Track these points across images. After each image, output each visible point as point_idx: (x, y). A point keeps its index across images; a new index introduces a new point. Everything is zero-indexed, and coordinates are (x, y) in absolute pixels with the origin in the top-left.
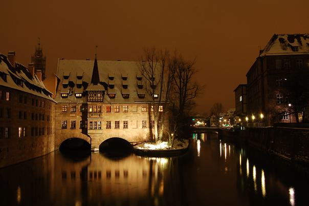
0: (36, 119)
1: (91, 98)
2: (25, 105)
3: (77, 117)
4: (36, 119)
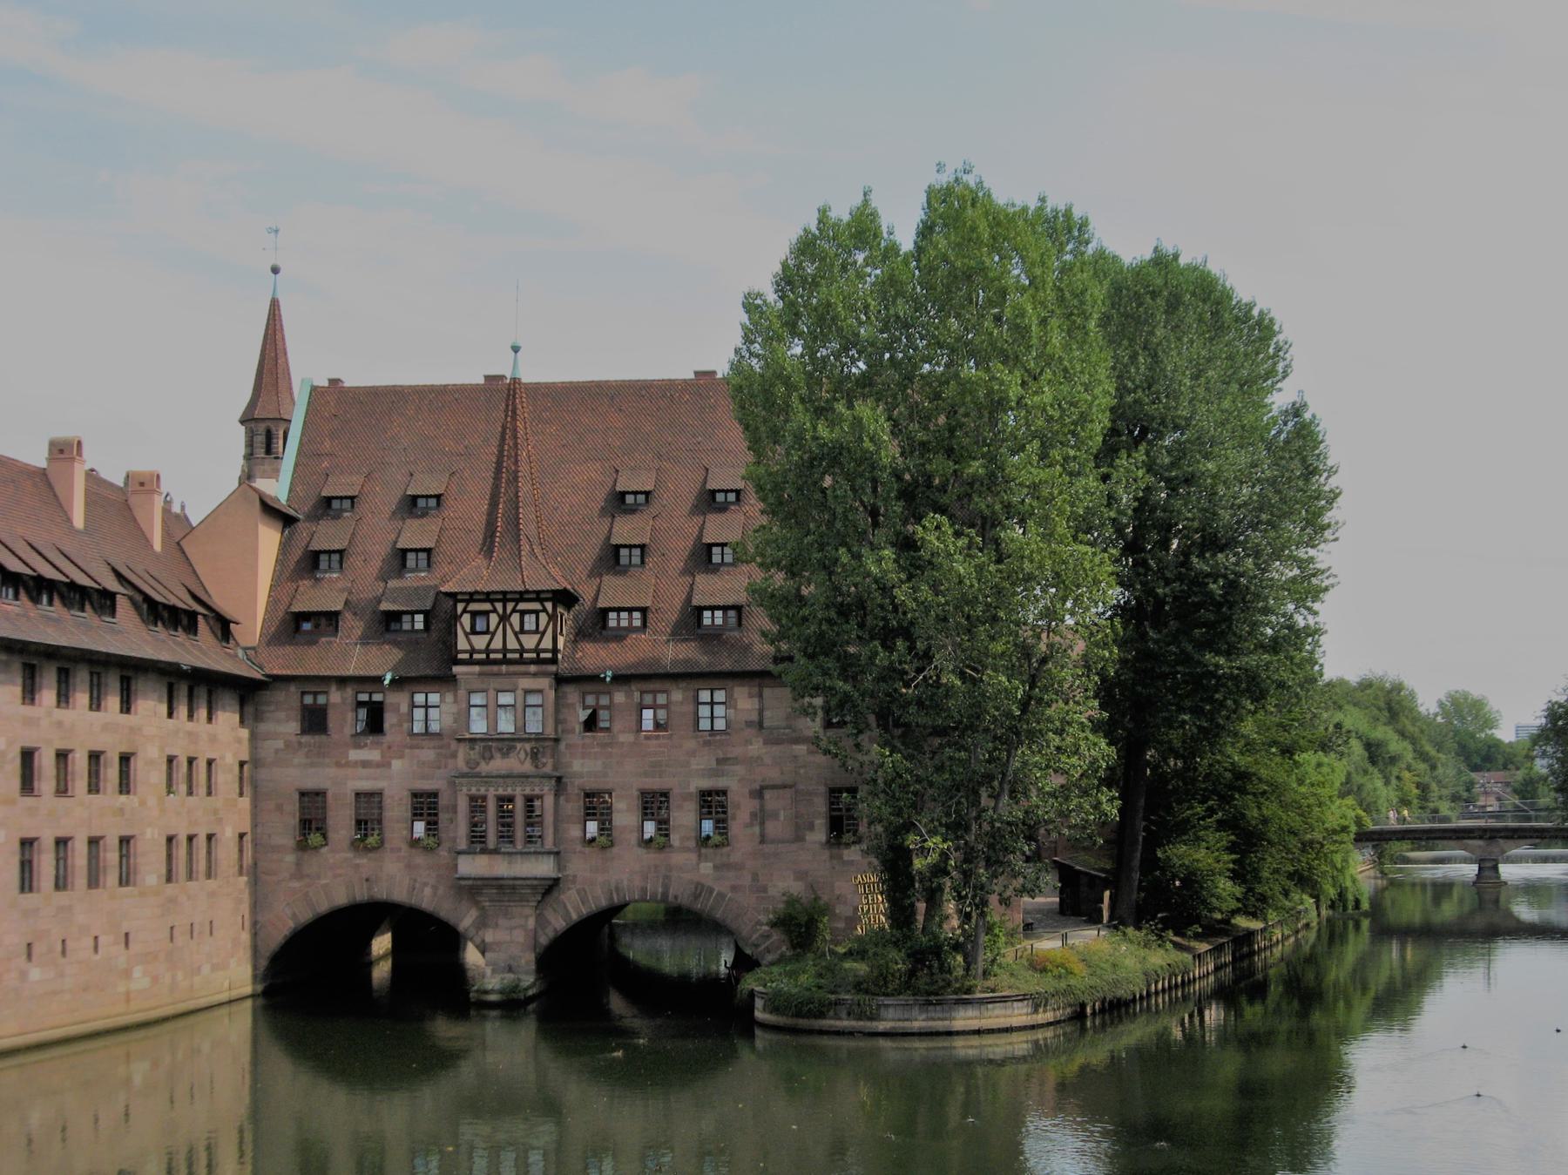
0: (62, 790)
1: (480, 642)
3: (397, 764)
4: (62, 790)
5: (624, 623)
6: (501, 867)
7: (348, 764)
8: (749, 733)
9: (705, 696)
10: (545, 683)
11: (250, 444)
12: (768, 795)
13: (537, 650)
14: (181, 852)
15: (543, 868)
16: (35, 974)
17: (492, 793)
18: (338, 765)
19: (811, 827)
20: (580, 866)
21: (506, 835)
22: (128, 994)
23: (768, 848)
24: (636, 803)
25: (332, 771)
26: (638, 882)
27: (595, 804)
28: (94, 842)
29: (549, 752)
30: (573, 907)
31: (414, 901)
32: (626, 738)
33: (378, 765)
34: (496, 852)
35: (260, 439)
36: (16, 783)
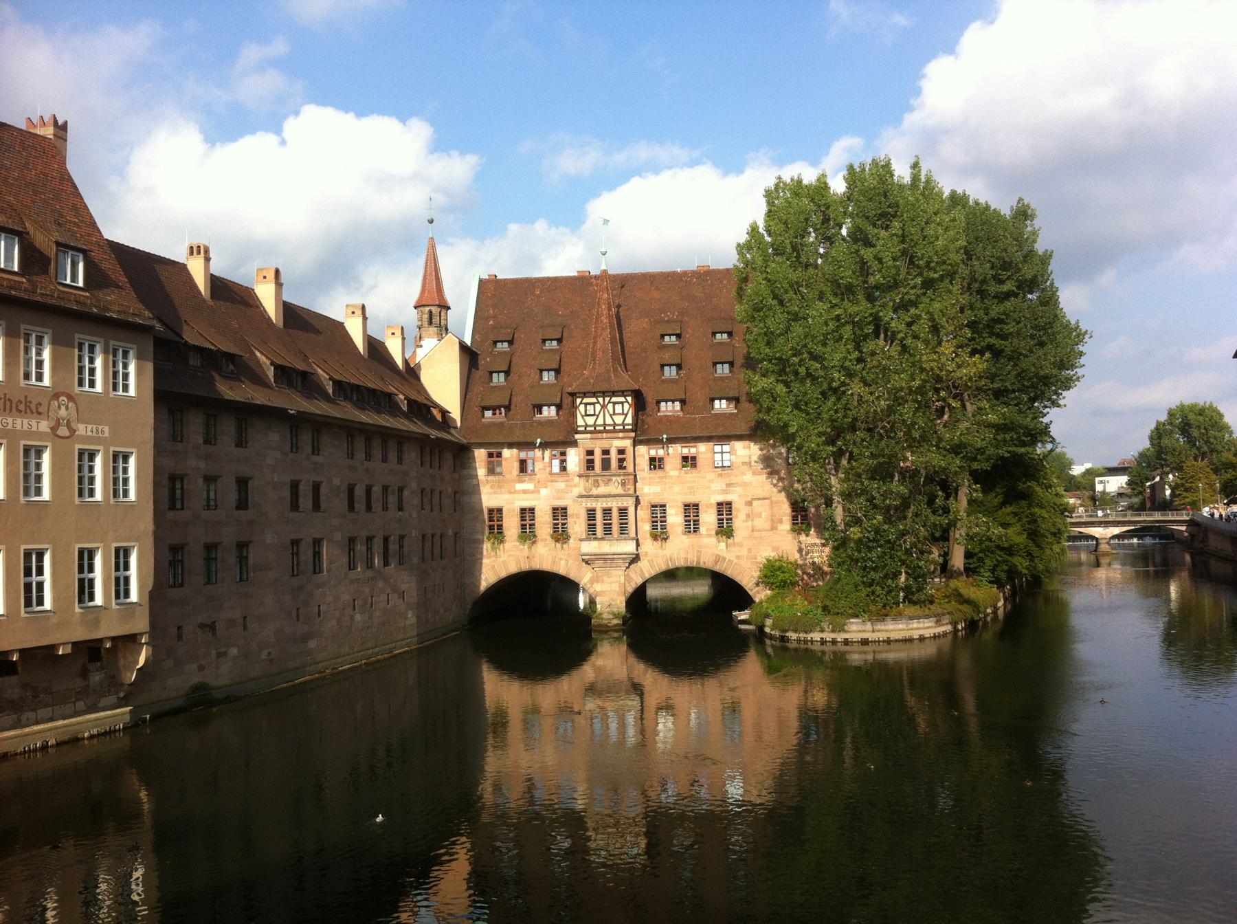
0: (369, 508)
1: (590, 421)
2: (314, 458)
3: (543, 491)
4: (369, 508)
5: (670, 408)
6: (606, 547)
7: (516, 492)
8: (746, 467)
9: (718, 448)
10: (627, 443)
11: (421, 319)
12: (755, 503)
13: (623, 425)
14: (428, 544)
15: (630, 547)
16: (358, 617)
17: (599, 505)
18: (510, 492)
19: (781, 521)
20: (648, 546)
21: (608, 530)
22: (405, 627)
23: (756, 534)
24: (681, 509)
25: (506, 496)
26: (683, 555)
27: (658, 511)
28: (386, 540)
29: (632, 481)
30: (646, 569)
31: (555, 569)
32: (675, 473)
33: (533, 492)
34: (602, 539)
35: (426, 317)
36: (346, 504)
